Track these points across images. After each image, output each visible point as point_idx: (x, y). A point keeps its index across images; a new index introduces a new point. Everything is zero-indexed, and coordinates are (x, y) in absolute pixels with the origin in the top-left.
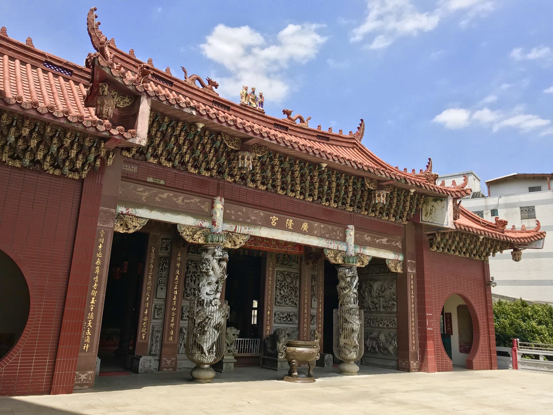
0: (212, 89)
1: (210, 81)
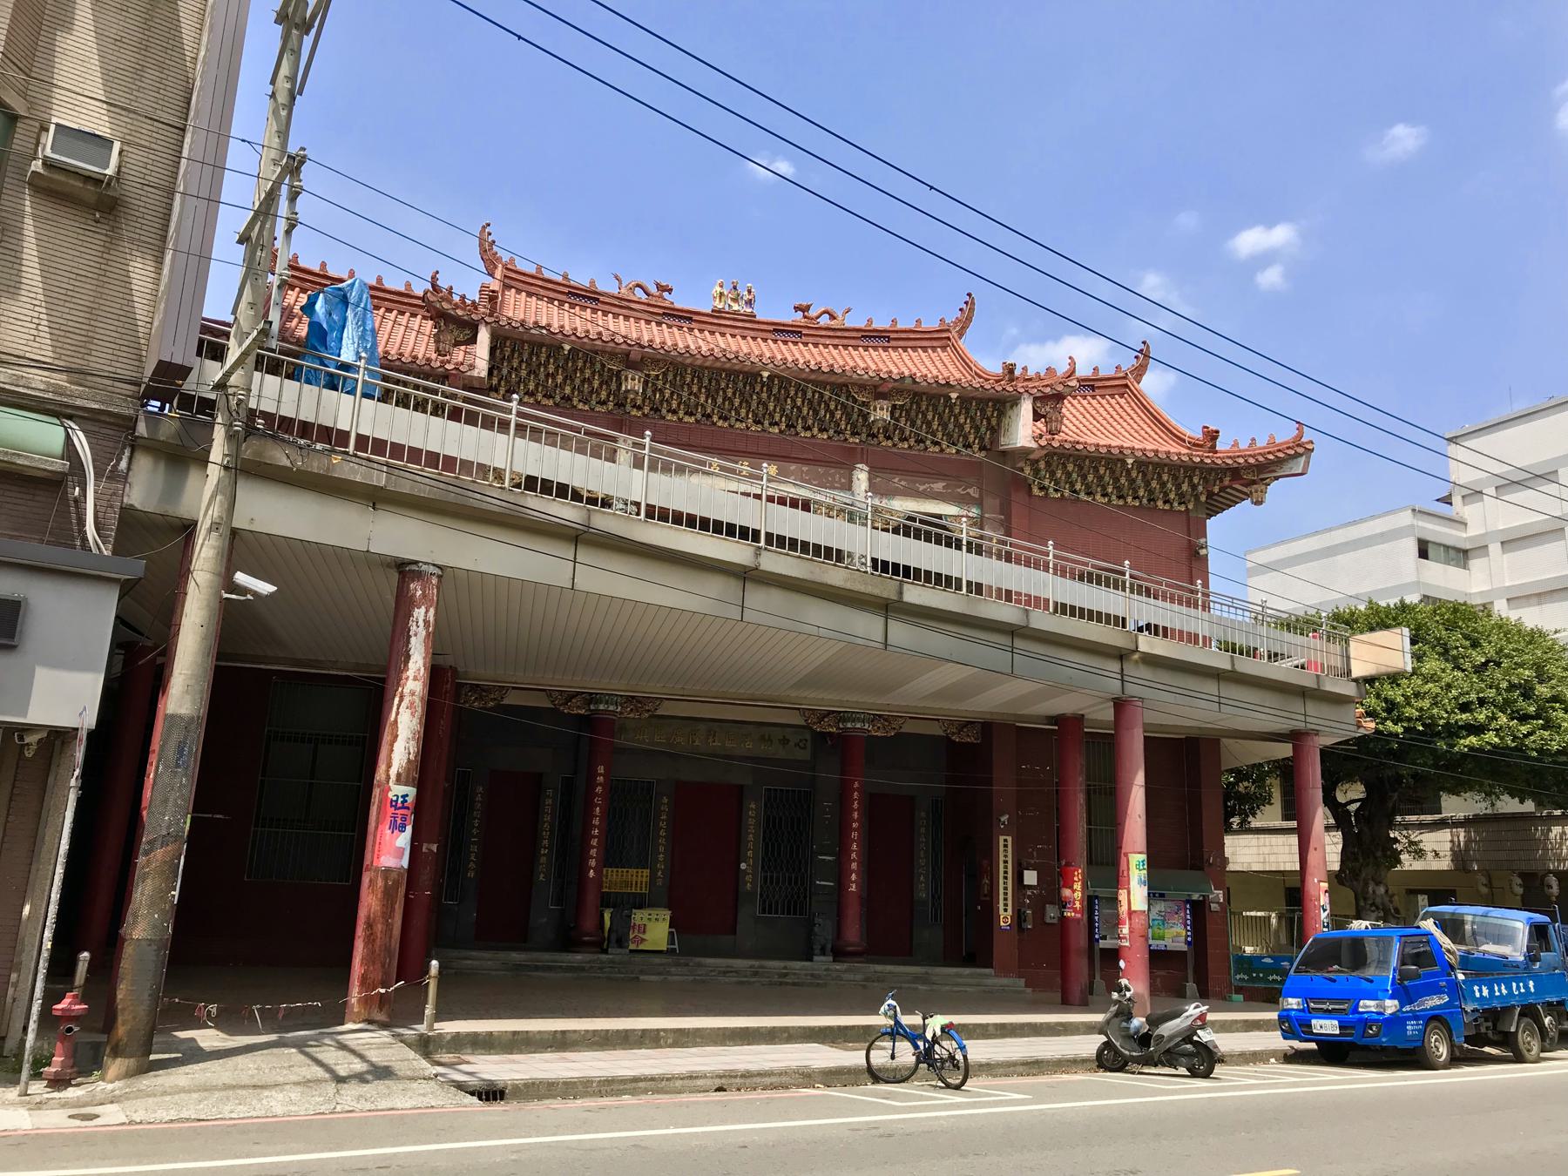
0: (661, 297)
1: (658, 286)
